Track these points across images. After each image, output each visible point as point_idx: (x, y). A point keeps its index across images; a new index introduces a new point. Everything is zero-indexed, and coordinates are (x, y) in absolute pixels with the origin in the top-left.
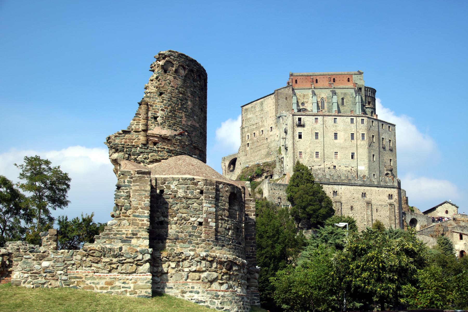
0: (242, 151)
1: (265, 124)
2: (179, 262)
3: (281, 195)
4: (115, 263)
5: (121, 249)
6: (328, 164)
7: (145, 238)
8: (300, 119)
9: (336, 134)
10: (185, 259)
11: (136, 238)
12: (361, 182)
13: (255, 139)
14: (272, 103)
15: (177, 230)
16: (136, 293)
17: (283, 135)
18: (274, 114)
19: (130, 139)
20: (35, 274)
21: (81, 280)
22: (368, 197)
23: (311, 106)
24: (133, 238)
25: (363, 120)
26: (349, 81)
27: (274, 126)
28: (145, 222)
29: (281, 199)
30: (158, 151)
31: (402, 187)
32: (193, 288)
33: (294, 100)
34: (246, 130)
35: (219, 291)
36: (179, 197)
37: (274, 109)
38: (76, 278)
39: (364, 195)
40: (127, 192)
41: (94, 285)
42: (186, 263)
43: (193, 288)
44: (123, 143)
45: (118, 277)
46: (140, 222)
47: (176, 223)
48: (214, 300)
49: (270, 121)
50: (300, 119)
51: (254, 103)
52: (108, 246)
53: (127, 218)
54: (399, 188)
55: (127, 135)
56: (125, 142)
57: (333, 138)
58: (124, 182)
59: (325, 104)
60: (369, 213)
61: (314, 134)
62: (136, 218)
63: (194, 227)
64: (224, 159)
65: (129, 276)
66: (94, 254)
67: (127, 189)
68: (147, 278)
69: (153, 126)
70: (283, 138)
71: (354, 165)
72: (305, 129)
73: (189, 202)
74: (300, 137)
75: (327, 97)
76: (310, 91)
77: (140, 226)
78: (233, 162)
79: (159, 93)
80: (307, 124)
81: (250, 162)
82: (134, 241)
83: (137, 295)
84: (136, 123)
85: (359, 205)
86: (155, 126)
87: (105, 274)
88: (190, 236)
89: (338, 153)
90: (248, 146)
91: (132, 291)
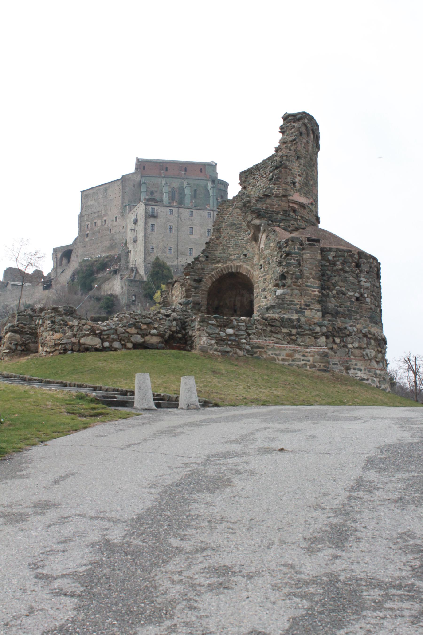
0: (80, 242)
1: (109, 213)
2: (343, 337)
3: (136, 292)
4: (294, 335)
5: (298, 320)
7: (318, 311)
10: (349, 335)
11: (309, 309)
13: (96, 229)
15: (336, 304)
16: (315, 366)
17: (131, 225)
18: (120, 202)
19: (271, 205)
20: (220, 341)
21: (263, 350)
24: (306, 309)
26: (201, 172)
27: (119, 216)
28: (317, 293)
30: (298, 219)
32: (356, 365)
34: (86, 218)
35: (377, 369)
36: (337, 270)
37: (121, 197)
38: (258, 347)
40: (297, 260)
41: (275, 357)
42: (349, 339)
43: (356, 365)
44: (264, 208)
45: (297, 349)
46: (313, 293)
47: (334, 297)
48: (375, 379)
49: (115, 210)
51: (97, 188)
52: (286, 316)
53: (298, 288)
55: (268, 200)
56: (267, 208)
57: (189, 233)
58: (295, 249)
59: (176, 195)
61: (169, 227)
62: (309, 288)
63: (352, 302)
64: (55, 250)
65: (307, 348)
66: (274, 324)
67: (297, 257)
68: (324, 352)
69: (292, 192)
70: (131, 230)
72: (159, 220)
73: (347, 275)
74: (153, 230)
77: (312, 296)
79: (296, 157)
82: (308, 313)
83: (317, 368)
84: (276, 188)
86: (294, 192)
87: (285, 346)
88: (349, 311)
89: (194, 250)
90: (87, 237)
91: (311, 364)
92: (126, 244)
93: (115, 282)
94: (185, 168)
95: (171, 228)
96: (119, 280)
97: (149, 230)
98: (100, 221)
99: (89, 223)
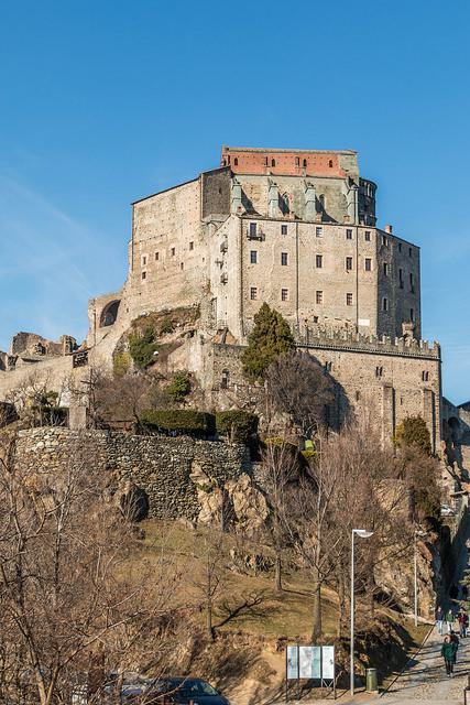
8: (253, 225)
9: (319, 258)
13: (158, 263)
14: (193, 196)
17: (220, 256)
23: (265, 203)
25: (367, 234)
26: (331, 166)
27: (196, 241)
29: (227, 373)
34: (141, 247)
37: (199, 209)
39: (379, 372)
50: (253, 225)
60: (390, 405)
74: (253, 260)
75: (295, 193)
76: (264, 182)
78: (111, 312)
81: (147, 306)
85: (371, 389)
89: (323, 294)
90: (144, 277)
92: (209, 286)
93: (192, 349)
95: (284, 256)
96: (199, 346)
97: (247, 261)
98: (164, 250)
99: (147, 255)
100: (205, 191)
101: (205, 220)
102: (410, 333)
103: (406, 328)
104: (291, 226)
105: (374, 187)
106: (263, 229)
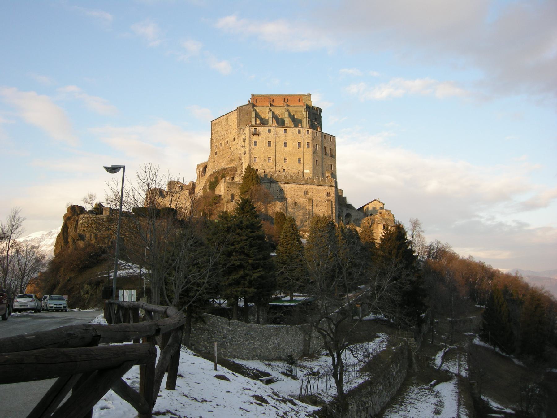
1: (229, 135)
6: (279, 168)
9: (285, 143)
12: (304, 182)
17: (243, 144)
22: (310, 194)
25: (308, 131)
27: (236, 137)
31: (339, 187)
33: (253, 115)
39: (306, 193)
49: (234, 133)
54: (336, 187)
71: (300, 168)
72: (260, 137)
75: (281, 114)
80: (262, 133)
94: (286, 99)
95: (269, 143)
97: (253, 145)
99: (217, 144)
100: (239, 115)
101: (240, 127)
102: (330, 175)
103: (327, 174)
104: (272, 129)
105: (320, 110)
106: (260, 131)
